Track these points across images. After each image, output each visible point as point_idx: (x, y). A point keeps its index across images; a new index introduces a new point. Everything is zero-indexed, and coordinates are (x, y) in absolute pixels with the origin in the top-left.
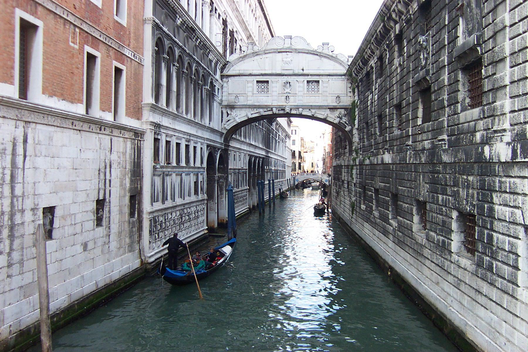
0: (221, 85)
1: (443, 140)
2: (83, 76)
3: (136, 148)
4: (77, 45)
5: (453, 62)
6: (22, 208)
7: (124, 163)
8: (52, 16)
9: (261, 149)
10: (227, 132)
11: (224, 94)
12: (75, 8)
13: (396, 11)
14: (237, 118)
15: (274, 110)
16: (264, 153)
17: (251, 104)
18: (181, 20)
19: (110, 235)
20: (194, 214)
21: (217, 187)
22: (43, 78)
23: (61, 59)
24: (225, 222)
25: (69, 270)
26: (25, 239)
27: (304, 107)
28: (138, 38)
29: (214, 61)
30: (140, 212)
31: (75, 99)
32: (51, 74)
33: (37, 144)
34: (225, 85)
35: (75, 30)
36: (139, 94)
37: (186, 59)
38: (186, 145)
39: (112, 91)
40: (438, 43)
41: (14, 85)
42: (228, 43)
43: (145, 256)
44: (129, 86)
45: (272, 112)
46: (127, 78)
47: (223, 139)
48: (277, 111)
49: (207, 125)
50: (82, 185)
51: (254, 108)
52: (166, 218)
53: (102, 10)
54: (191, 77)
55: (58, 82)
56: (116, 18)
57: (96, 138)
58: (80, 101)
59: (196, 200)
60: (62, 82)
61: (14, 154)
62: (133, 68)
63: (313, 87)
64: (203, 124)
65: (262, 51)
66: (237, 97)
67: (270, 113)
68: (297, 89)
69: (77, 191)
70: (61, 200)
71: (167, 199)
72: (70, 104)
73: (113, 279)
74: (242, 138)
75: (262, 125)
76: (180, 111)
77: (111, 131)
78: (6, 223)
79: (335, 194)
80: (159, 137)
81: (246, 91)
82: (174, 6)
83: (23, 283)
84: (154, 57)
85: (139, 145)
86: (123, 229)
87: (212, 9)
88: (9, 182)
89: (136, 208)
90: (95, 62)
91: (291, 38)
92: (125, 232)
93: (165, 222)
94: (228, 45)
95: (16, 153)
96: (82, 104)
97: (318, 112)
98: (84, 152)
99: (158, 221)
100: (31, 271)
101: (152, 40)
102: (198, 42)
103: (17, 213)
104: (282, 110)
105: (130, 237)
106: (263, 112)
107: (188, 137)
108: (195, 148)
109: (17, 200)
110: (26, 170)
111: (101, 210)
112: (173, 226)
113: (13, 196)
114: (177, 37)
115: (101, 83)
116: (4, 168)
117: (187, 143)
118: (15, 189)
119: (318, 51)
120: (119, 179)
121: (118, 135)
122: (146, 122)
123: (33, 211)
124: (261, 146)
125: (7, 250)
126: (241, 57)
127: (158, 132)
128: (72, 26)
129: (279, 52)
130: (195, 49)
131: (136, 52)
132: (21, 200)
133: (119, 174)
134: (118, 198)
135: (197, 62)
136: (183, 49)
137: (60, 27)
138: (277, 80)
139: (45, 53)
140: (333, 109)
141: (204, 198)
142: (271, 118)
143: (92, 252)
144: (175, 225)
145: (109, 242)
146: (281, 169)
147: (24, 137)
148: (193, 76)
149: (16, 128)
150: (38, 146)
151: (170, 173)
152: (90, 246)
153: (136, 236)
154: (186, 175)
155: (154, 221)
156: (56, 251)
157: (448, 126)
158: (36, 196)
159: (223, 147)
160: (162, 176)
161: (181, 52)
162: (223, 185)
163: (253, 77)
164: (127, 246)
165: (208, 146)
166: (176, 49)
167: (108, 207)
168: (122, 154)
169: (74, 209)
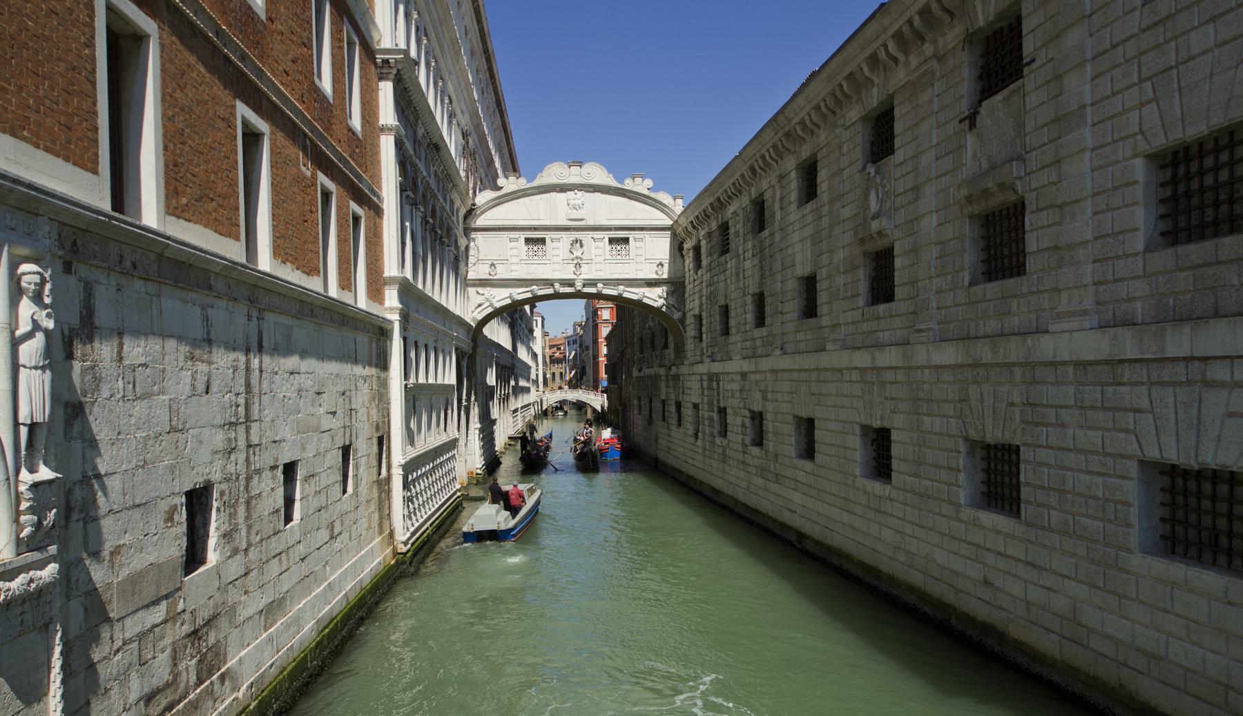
1: (933, 329)
5: (950, 205)
10: (477, 325)
13: (808, 122)
14: (494, 301)
15: (557, 285)
17: (517, 277)
18: (423, 130)
22: (273, 230)
24: (474, 474)
27: (608, 282)
33: (274, 349)
39: (349, 253)
40: (912, 174)
47: (471, 336)
50: (328, 422)
53: (332, 106)
54: (436, 232)
63: (619, 248)
66: (493, 265)
67: (550, 291)
68: (593, 249)
70: (303, 449)
72: (305, 276)
80: (407, 335)
96: (319, 276)
105: (380, 508)
109: (254, 454)
113: (249, 446)
116: (237, 395)
119: (625, 187)
122: (392, 309)
133: (366, 399)
134: (365, 442)
138: (559, 236)
140: (651, 283)
147: (258, 336)
149: (249, 320)
157: (938, 309)
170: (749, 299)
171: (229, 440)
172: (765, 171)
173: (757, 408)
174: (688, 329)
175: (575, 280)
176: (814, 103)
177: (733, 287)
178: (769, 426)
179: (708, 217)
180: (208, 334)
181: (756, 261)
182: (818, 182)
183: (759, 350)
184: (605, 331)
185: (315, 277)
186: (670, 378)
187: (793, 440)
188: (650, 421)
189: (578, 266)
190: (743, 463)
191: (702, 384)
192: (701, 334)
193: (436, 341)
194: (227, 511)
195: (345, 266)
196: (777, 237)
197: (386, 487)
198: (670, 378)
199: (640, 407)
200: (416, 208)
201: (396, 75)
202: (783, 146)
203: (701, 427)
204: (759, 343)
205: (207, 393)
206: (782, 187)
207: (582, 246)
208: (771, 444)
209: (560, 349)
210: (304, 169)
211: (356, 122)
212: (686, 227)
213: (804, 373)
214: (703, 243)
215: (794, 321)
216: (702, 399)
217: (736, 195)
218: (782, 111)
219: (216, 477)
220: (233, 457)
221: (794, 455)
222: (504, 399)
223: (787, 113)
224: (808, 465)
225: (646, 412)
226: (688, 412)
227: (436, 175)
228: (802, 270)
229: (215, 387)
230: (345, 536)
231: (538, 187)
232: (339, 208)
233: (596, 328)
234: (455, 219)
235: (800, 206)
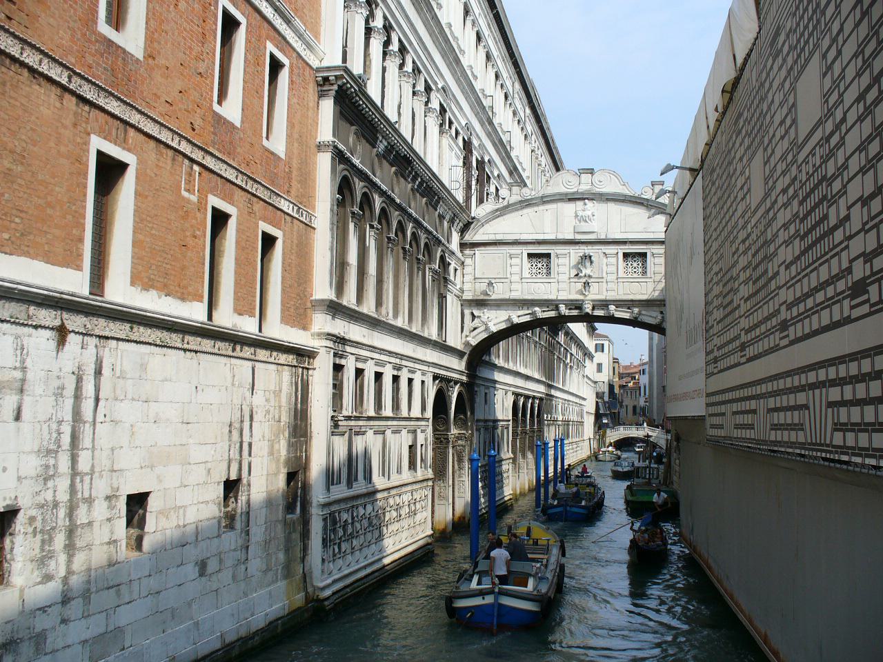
0: (460, 262)
3: (300, 382)
4: (194, 195)
6: (91, 495)
7: (277, 411)
8: (152, 144)
9: (538, 381)
10: (471, 351)
11: (467, 278)
12: (194, 130)
15: (563, 308)
16: (542, 388)
17: (517, 298)
18: (386, 144)
19: (248, 547)
20: (407, 508)
21: (453, 455)
22: (133, 257)
23: (165, 220)
25: (173, 612)
26: (93, 552)
27: (620, 304)
28: (306, 179)
29: (448, 217)
31: (189, 294)
32: (147, 250)
33: (119, 377)
34: (468, 261)
35: (192, 168)
36: (306, 282)
37: (395, 216)
38: (393, 375)
39: (256, 277)
41: (81, 270)
42: (474, 183)
43: (313, 586)
44: (288, 268)
45: (557, 312)
46: (284, 254)
48: (567, 311)
49: (434, 337)
50: (197, 454)
52: (355, 514)
54: (404, 249)
55: (159, 264)
56: (265, 142)
57: (226, 364)
58: (200, 300)
60: (166, 264)
61: (78, 396)
62: (295, 233)
63: (635, 264)
64: (426, 335)
65: (536, 198)
66: (490, 284)
67: (552, 314)
68: (605, 268)
69: (190, 464)
70: (161, 481)
71: (356, 479)
72: (181, 302)
73: (254, 629)
74: (501, 361)
75: (539, 336)
76: (384, 311)
77: (253, 353)
78: (60, 523)
80: (343, 362)
82: (373, 119)
83: (87, 635)
84: (335, 212)
85: (305, 377)
86: (273, 535)
87: (444, 120)
88: (69, 448)
89: (298, 496)
92: (276, 541)
93: (353, 523)
94: (473, 187)
95: (82, 394)
96: (202, 302)
97: (643, 312)
98: (203, 390)
99: (340, 520)
100: (103, 612)
101: (332, 181)
102: (417, 182)
103: (80, 504)
104: (576, 308)
105: (287, 550)
106: (541, 313)
107: (398, 361)
108: (410, 381)
109: (82, 481)
110: (98, 425)
111: (233, 500)
112: (368, 530)
113: (75, 473)
114: (377, 175)
116: (60, 422)
117: (395, 373)
118: (78, 461)
120: (266, 442)
121: (266, 360)
122: (319, 335)
123: (110, 501)
124: (537, 376)
125: (62, 572)
126: (497, 210)
127: (340, 353)
128: (186, 162)
129: (570, 200)
130: (411, 197)
131: (301, 203)
132: (89, 481)
134: (264, 478)
135: (416, 222)
136: (389, 197)
137: (166, 163)
139: (137, 211)
141: (426, 477)
142: (556, 325)
143: (214, 578)
144: (371, 528)
145: (247, 559)
146: (575, 419)
148: (408, 247)
149: (82, 348)
150: (120, 380)
151: (364, 430)
152: (212, 566)
154: (394, 432)
155: (331, 522)
156: (150, 575)
158: (114, 473)
159: (464, 378)
160: (347, 435)
161: (383, 202)
162: (464, 451)
164: (280, 567)
165: (435, 377)
166: (376, 197)
167: (246, 493)
168: (272, 395)
169: (185, 497)
171: (47, 467)
175: (583, 301)
180: (23, 361)
185: (196, 304)
189: (586, 284)
193: (398, 368)
194: (39, 537)
205: (18, 418)
207: (591, 262)
209: (635, 377)
219: (23, 502)
220: (50, 484)
229: (26, 414)
232: (239, 231)
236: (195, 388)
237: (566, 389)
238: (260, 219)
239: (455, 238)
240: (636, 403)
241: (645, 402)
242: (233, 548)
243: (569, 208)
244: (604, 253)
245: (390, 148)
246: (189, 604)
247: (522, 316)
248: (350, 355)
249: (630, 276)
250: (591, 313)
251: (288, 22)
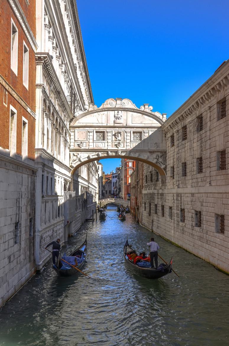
2: (9, 128)
13: (222, 84)
15: (110, 153)
16: (87, 184)
24: (71, 235)
30: (34, 232)
31: (6, 146)
34: (72, 134)
47: (70, 174)
51: (94, 152)
54: (57, 129)
59: (59, 220)
79: (145, 214)
80: (43, 174)
81: (88, 139)
90: (13, 117)
91: (121, 100)
105: (30, 251)
106: (101, 154)
115: (17, 133)
119: (140, 110)
120: (25, 207)
121: (25, 173)
127: (43, 170)
128: (4, 90)
129: (112, 110)
136: (55, 108)
140: (152, 152)
143: (12, 263)
153: (32, 250)
159: (70, 180)
163: (93, 128)
164: (28, 258)
165: (65, 180)
170: (195, 160)
172: (203, 104)
173: (198, 210)
174: (168, 173)
175: (117, 150)
176: (225, 76)
177: (188, 155)
178: (204, 217)
179: (177, 123)
181: (199, 143)
182: (226, 110)
183: (200, 183)
184: (130, 172)
186: (159, 195)
187: (214, 225)
188: (150, 215)
190: (192, 234)
191: (174, 198)
192: (174, 175)
195: (19, 145)
196: (208, 133)
197: (33, 241)
198: (159, 195)
199: (145, 207)
200: (49, 119)
201: (43, 64)
202: (211, 94)
203: (173, 217)
204: (200, 180)
206: (210, 112)
207: (121, 135)
208: (205, 226)
209: (110, 179)
210: (4, 104)
211: (26, 85)
212: (167, 127)
213: (220, 194)
214: (175, 134)
215: (216, 171)
216: (174, 205)
217: (190, 114)
218: (210, 79)
221: (215, 231)
222: (84, 202)
223: (213, 80)
224: (221, 236)
225: (148, 210)
226: (167, 210)
227: (58, 105)
228: (220, 148)
230: (15, 261)
231: (102, 109)
233: (126, 170)
234: (65, 123)
235: (218, 120)
236: (8, 185)
237: (92, 183)
238: (23, 115)
239: (68, 124)
240: (110, 190)
241: (114, 189)
242: (17, 250)
243: (112, 113)
244: (126, 132)
245: (55, 88)
246: (6, 274)
247: (93, 155)
248: (45, 171)
249: (135, 140)
250: (120, 154)
251: (29, 32)
